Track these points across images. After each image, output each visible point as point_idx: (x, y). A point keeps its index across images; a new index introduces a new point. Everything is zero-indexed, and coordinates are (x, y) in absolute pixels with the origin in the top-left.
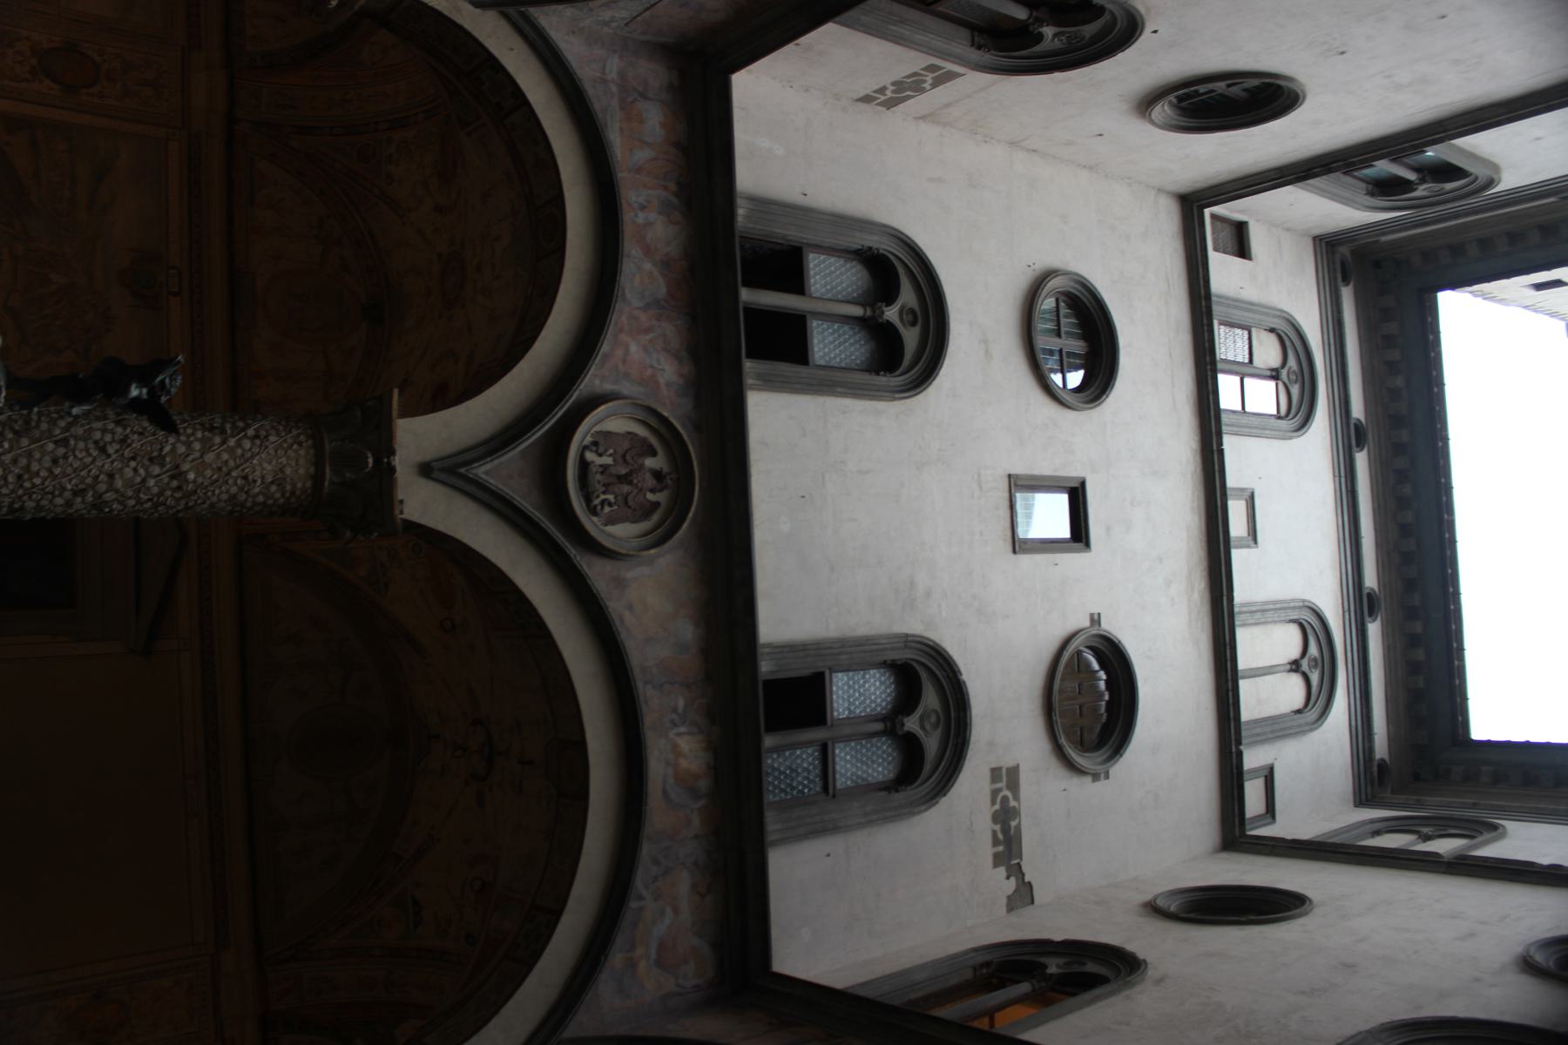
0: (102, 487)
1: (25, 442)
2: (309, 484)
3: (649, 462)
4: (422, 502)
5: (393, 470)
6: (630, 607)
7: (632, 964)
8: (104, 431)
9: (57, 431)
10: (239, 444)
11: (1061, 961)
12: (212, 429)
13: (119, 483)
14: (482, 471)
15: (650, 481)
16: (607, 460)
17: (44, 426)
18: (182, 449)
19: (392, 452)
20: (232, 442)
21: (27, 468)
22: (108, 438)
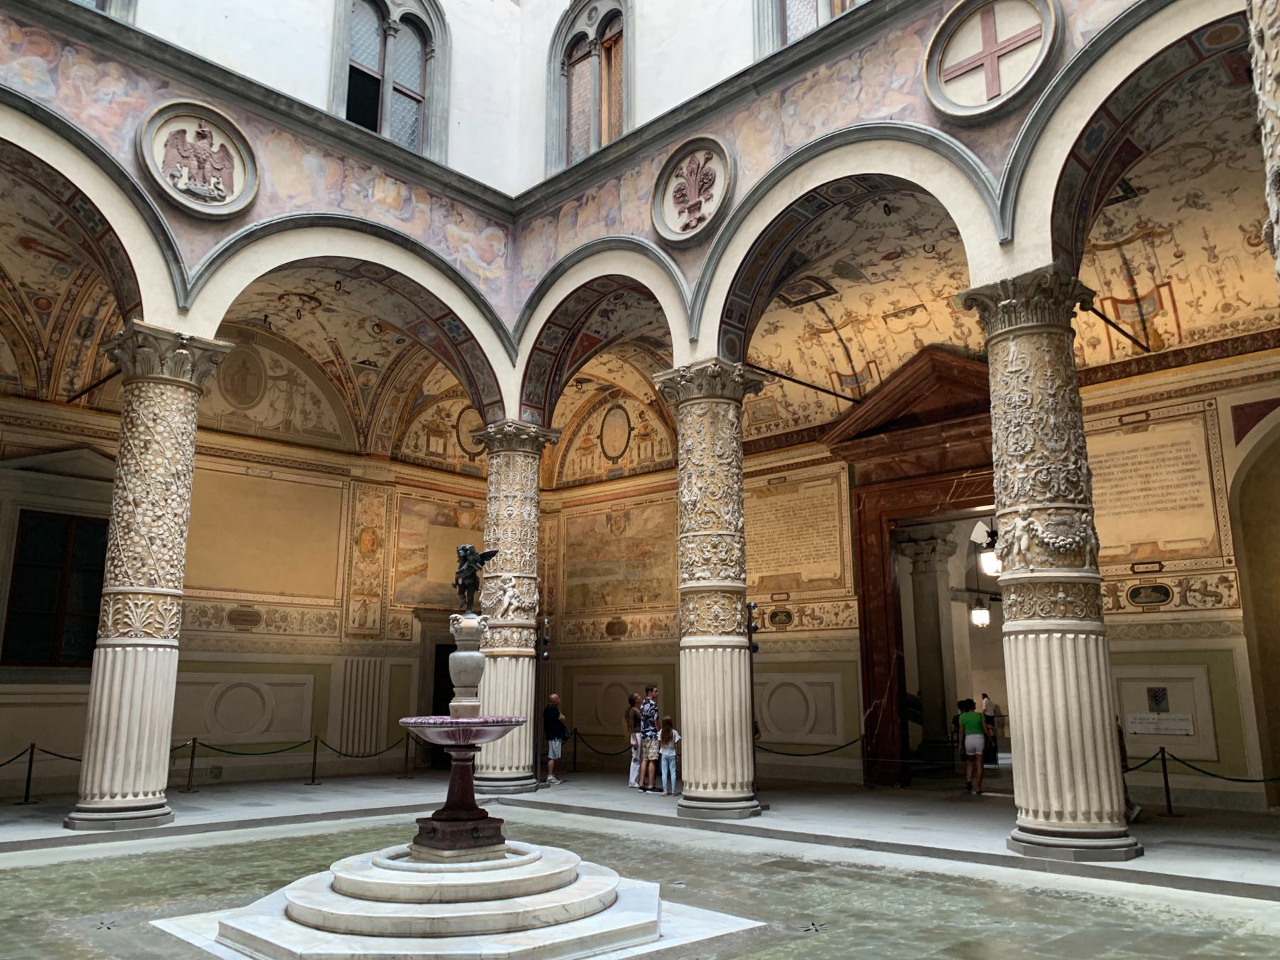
0: (181, 521)
1: (150, 562)
2: (189, 394)
3: (190, 138)
4: (203, 323)
5: (192, 339)
6: (291, 197)
7: (486, 280)
8: (144, 515)
9: (143, 542)
10: (160, 434)
11: (584, 18)
12: (145, 447)
13: (179, 511)
14: (192, 272)
15: (203, 143)
16: (185, 171)
17: (139, 549)
18: (161, 470)
19: (179, 336)
20: (158, 438)
21: (167, 562)
22: (150, 513)
